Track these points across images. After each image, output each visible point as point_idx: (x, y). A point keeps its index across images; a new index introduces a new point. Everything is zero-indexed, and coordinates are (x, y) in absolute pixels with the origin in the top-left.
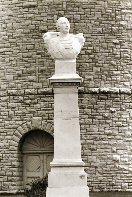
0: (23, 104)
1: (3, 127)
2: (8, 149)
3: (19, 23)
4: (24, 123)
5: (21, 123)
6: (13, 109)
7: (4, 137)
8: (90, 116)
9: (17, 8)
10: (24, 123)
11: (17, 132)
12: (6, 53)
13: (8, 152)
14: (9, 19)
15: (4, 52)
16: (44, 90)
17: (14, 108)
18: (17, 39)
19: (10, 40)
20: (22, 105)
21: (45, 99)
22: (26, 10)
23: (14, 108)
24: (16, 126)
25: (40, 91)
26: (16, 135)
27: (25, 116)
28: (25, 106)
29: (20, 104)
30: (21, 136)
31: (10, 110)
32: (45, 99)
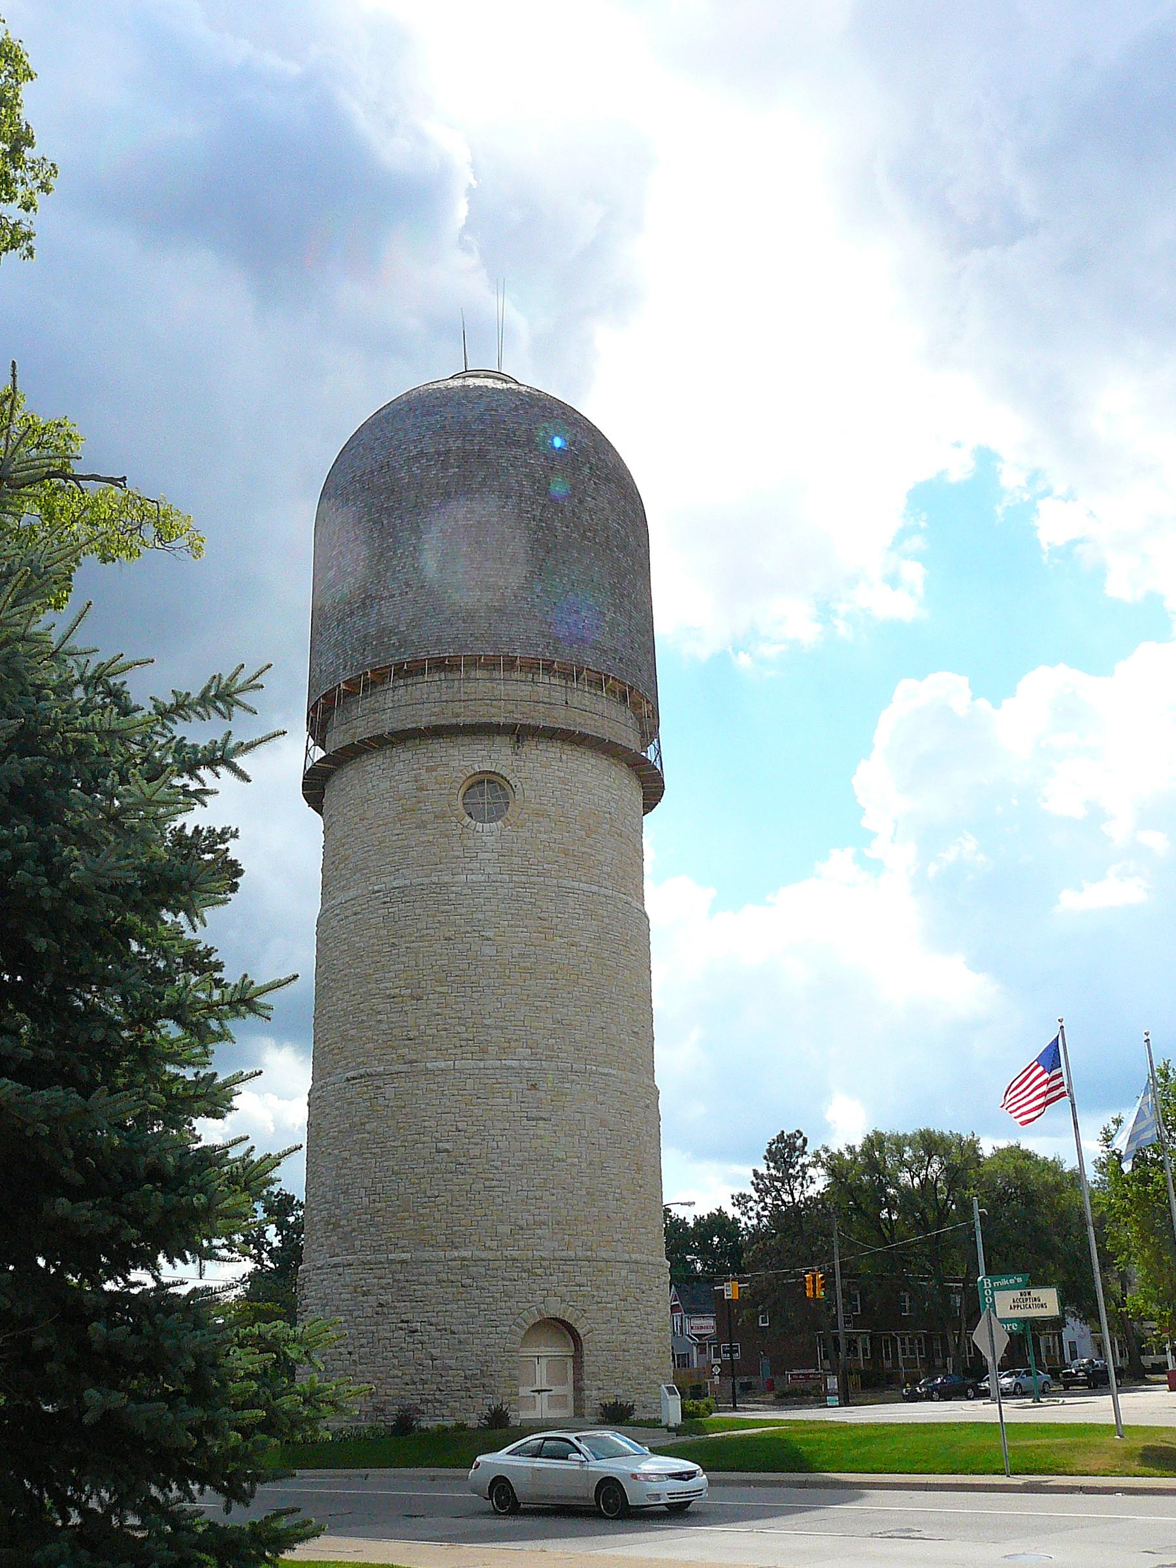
1: (494, 1313)
3: (521, 1142)
8: (622, 1298)
9: (516, 1118)
11: (519, 1320)
12: (496, 1189)
14: (502, 1136)
15: (494, 1187)
16: (564, 1254)
17: (515, 1280)
18: (518, 1168)
19: (506, 1169)
21: (565, 1268)
22: (534, 1123)
24: (517, 1311)
25: (558, 1254)
26: (518, 1325)
29: (525, 1275)
31: (505, 1283)
32: (565, 1268)
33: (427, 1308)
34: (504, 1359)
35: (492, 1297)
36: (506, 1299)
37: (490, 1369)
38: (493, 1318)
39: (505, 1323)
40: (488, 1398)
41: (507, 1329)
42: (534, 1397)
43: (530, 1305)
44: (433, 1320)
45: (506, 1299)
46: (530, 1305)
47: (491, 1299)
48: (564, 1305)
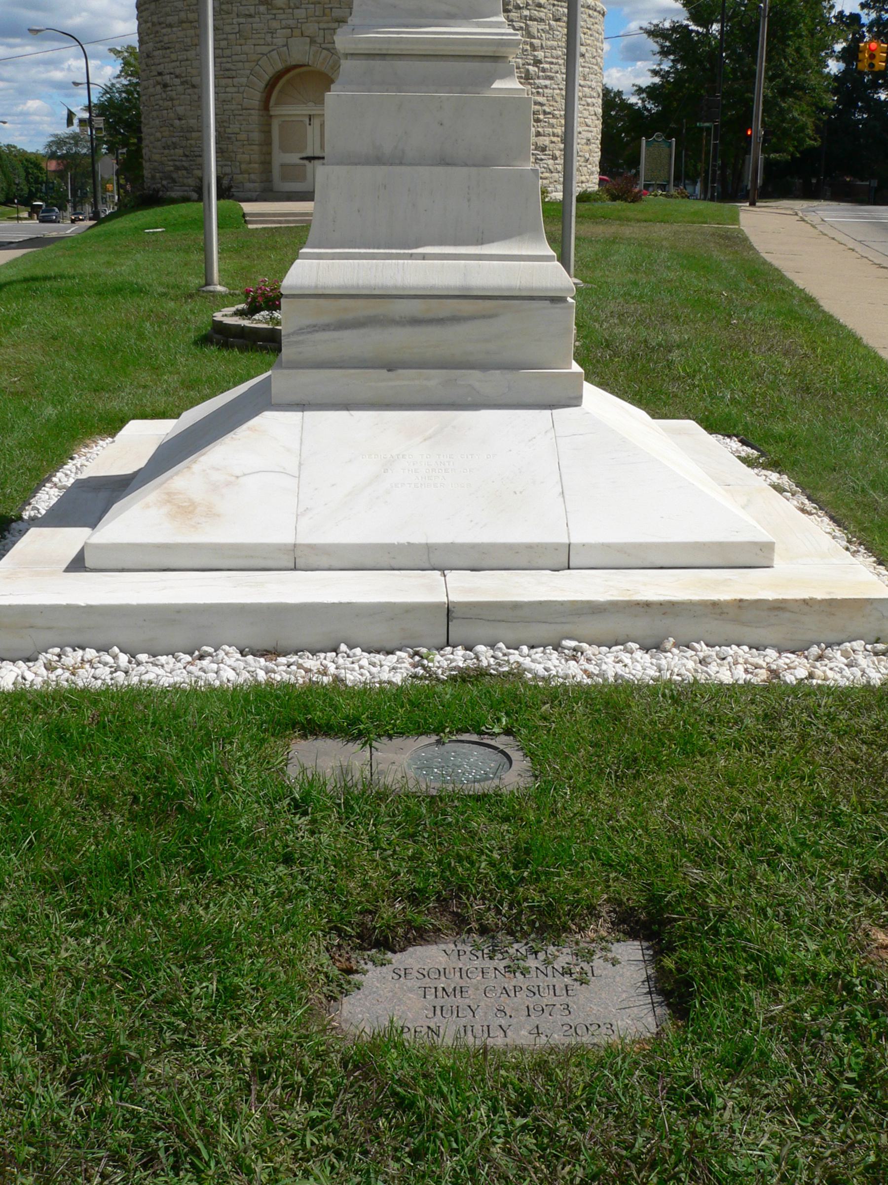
0: (270, 7)
1: (229, 60)
2: (240, 107)
4: (273, 50)
5: (265, 49)
6: (250, 20)
7: (230, 80)
10: (273, 50)
13: (241, 112)
17: (250, 16)
20: (268, 9)
23: (250, 16)
27: (274, 35)
28: (274, 12)
30: (267, 78)
31: (242, 20)
33: (174, 56)
34: (241, 118)
35: (225, 39)
36: (243, 41)
37: (228, 130)
38: (229, 66)
39: (241, 72)
40: (226, 165)
41: (244, 80)
42: (282, 165)
43: (270, 48)
44: (178, 71)
45: (243, 41)
46: (270, 48)
47: (225, 42)
48: (314, 48)
